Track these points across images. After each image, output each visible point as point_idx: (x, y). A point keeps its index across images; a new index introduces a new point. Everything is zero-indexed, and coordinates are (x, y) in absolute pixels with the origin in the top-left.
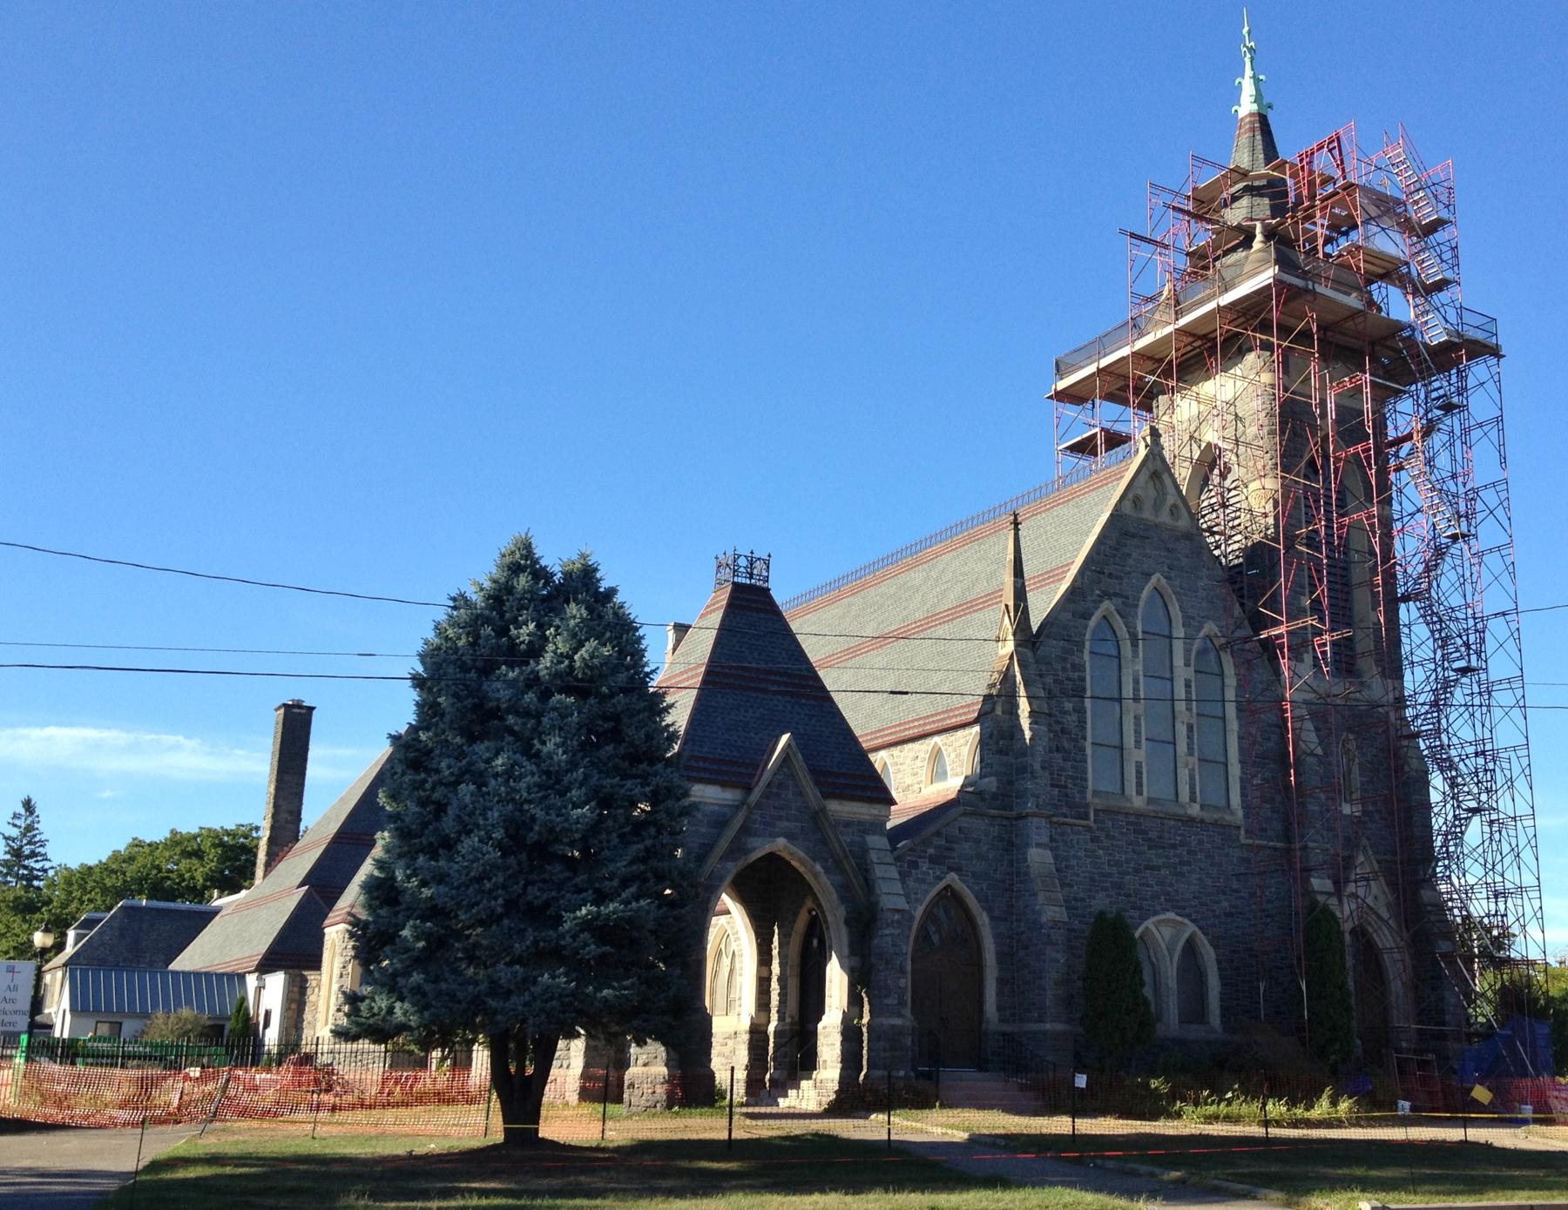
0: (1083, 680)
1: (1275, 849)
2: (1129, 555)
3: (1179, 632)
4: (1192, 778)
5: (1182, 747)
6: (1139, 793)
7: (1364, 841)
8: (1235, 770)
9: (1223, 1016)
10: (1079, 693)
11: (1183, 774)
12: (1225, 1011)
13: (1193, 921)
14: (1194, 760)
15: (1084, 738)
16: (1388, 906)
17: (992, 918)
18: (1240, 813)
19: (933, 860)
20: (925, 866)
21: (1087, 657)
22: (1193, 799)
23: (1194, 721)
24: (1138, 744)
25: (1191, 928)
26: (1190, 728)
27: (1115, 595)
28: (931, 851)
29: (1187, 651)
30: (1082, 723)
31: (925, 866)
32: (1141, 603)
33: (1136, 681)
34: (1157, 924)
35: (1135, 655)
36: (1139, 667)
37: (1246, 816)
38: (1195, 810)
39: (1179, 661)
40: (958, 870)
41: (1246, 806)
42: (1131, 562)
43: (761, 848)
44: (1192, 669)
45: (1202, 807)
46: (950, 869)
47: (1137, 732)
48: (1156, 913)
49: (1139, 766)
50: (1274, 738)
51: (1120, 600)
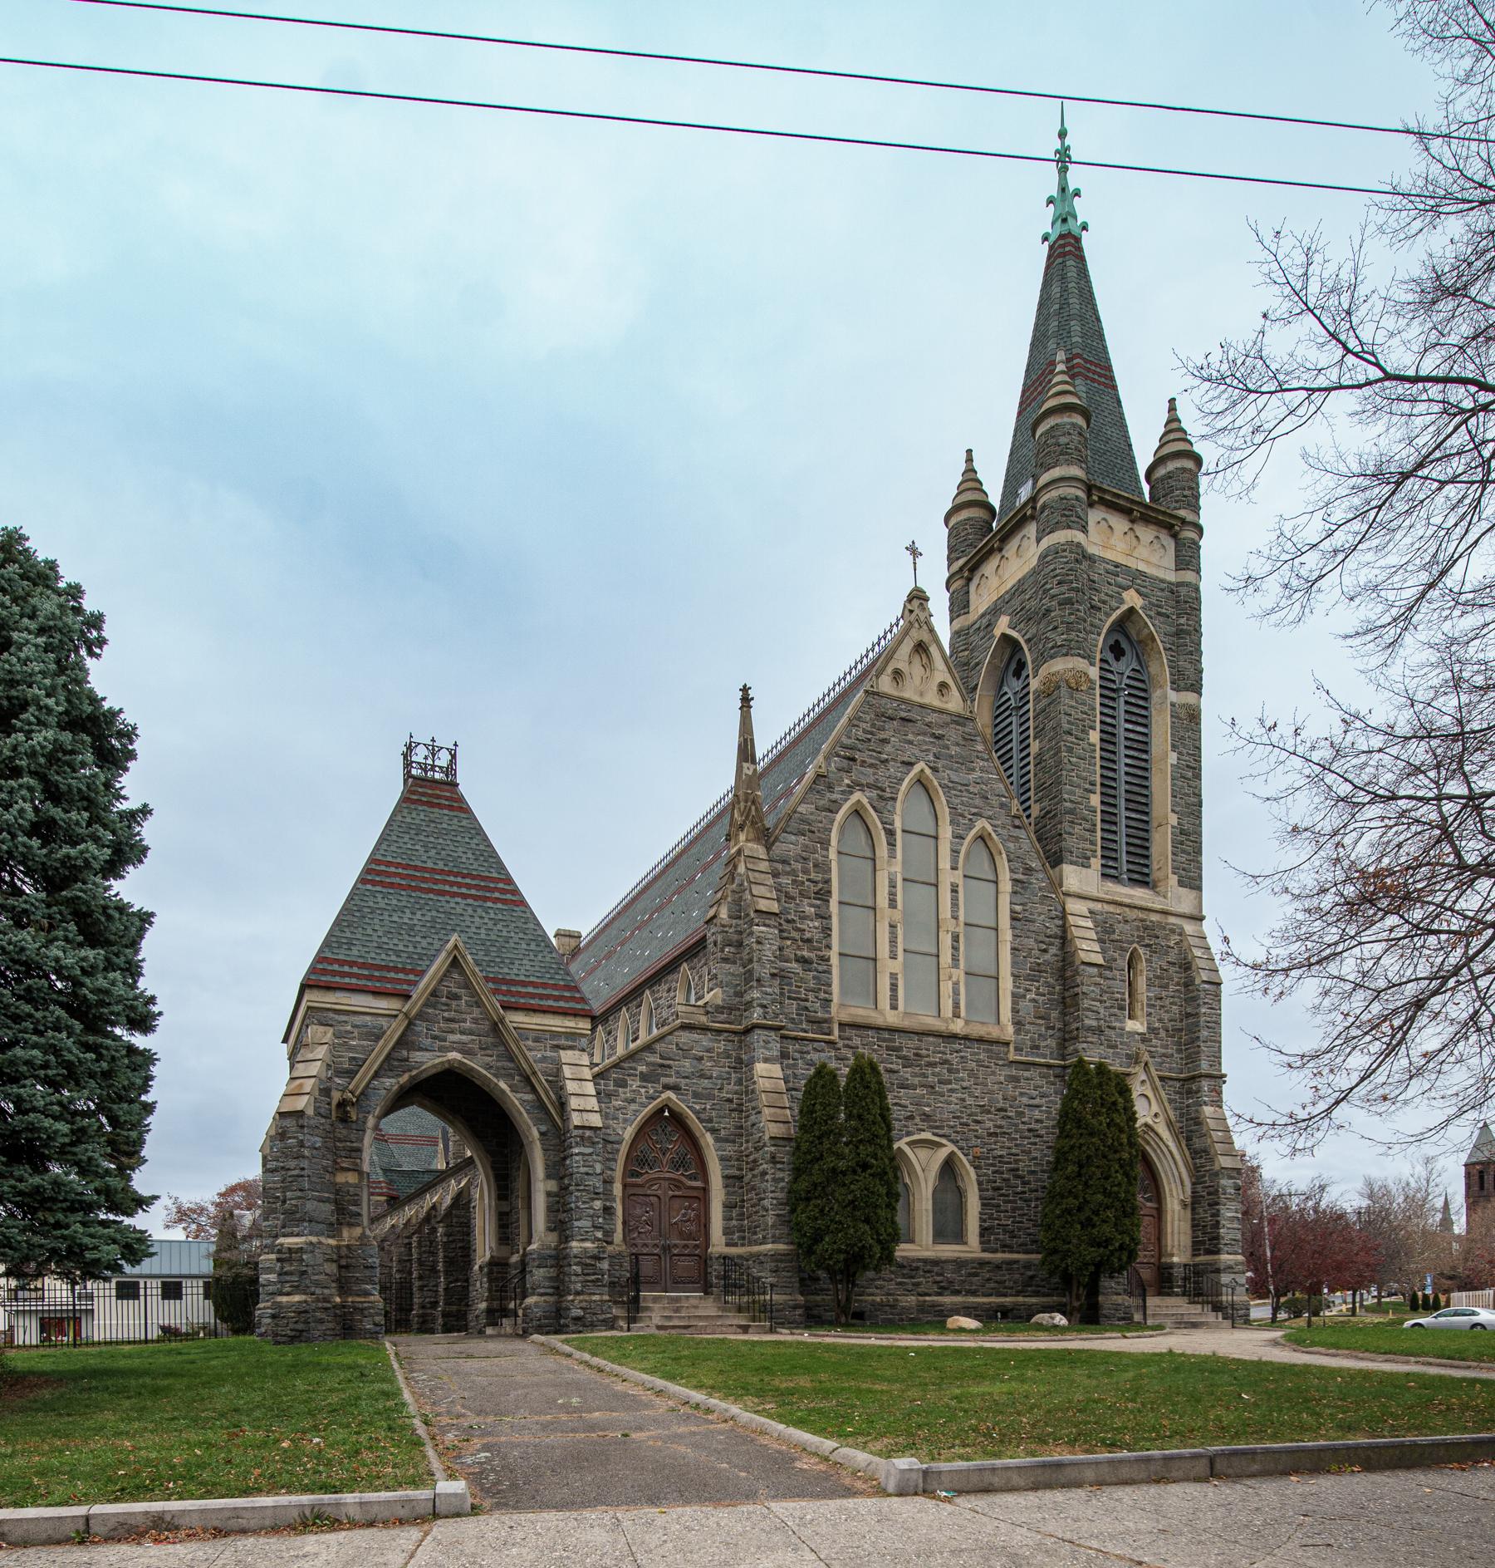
0: (828, 881)
1: (1049, 1066)
2: (885, 741)
3: (946, 832)
4: (956, 992)
5: (946, 958)
6: (894, 1007)
7: (1146, 1057)
8: (1007, 984)
9: (982, 1235)
10: (824, 895)
11: (947, 988)
12: (984, 1232)
13: (955, 1142)
14: (959, 974)
15: (829, 947)
16: (1169, 1124)
17: (717, 1140)
18: (1010, 1029)
19: (644, 1078)
20: (635, 1084)
21: (833, 855)
22: (956, 1015)
23: (961, 929)
24: (893, 957)
25: (951, 1147)
26: (956, 938)
27: (869, 786)
28: (643, 1068)
29: (955, 852)
30: (827, 931)
31: (635, 1084)
32: (900, 796)
33: (893, 885)
34: (908, 1144)
35: (892, 855)
36: (897, 868)
37: (1017, 1032)
38: (958, 1027)
39: (945, 863)
40: (675, 1088)
41: (1018, 1024)
42: (888, 748)
43: (428, 1060)
44: (960, 872)
45: (967, 1022)
46: (667, 1087)
47: (893, 942)
48: (908, 1134)
49: (893, 976)
50: (1053, 950)
51: (874, 793)
